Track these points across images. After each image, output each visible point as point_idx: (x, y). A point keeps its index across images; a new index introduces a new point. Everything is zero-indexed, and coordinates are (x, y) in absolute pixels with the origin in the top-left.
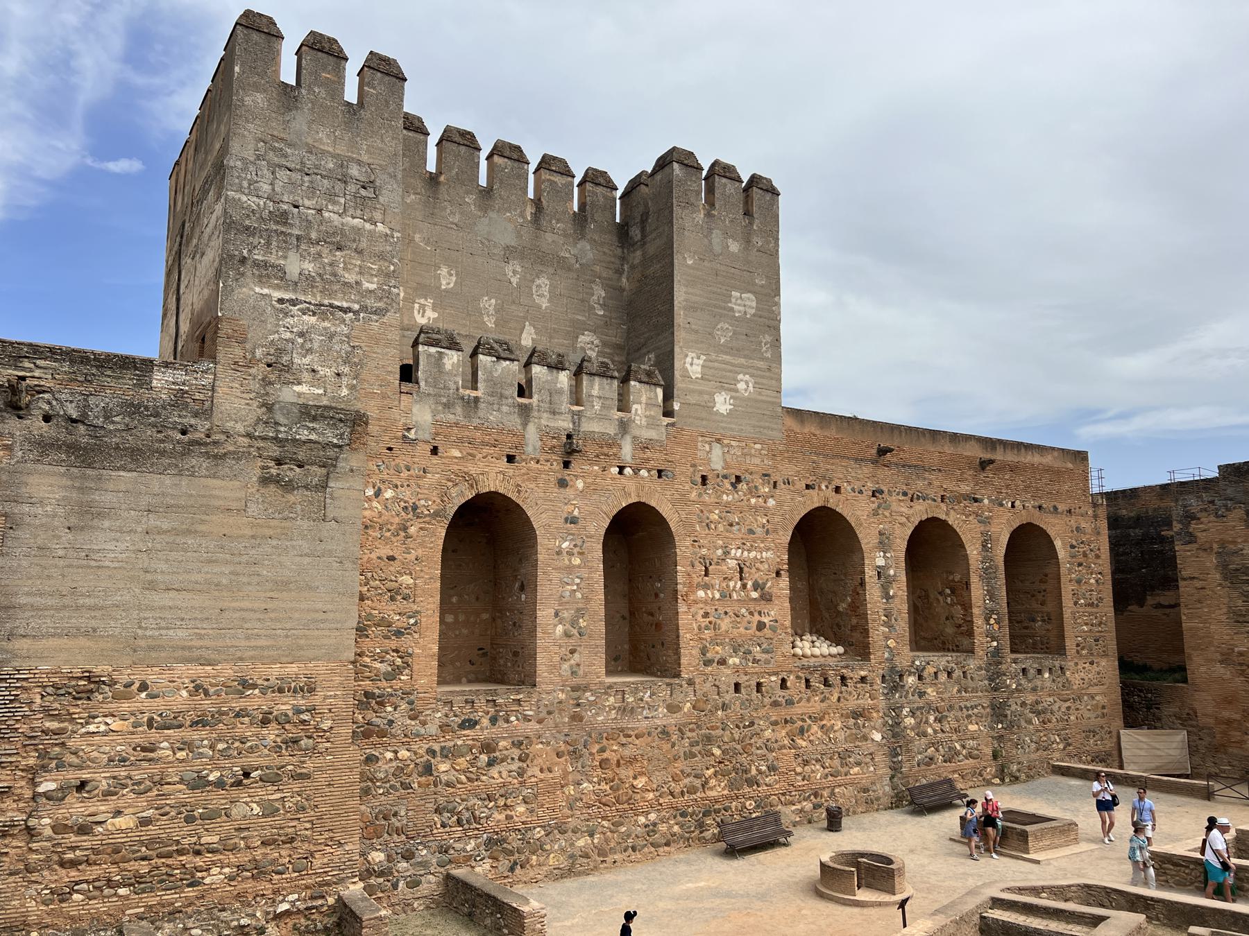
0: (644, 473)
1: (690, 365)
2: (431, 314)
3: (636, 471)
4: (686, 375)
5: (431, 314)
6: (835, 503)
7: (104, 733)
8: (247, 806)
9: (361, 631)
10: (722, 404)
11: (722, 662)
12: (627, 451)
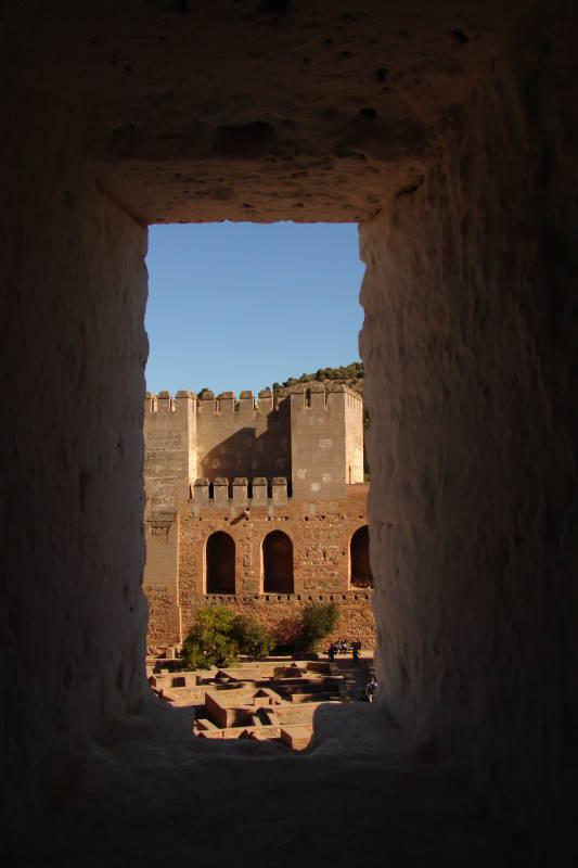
1: (299, 473)
2: (219, 464)
3: (275, 518)
4: (297, 478)
5: (219, 464)
10: (315, 487)
11: (313, 588)
12: (271, 512)
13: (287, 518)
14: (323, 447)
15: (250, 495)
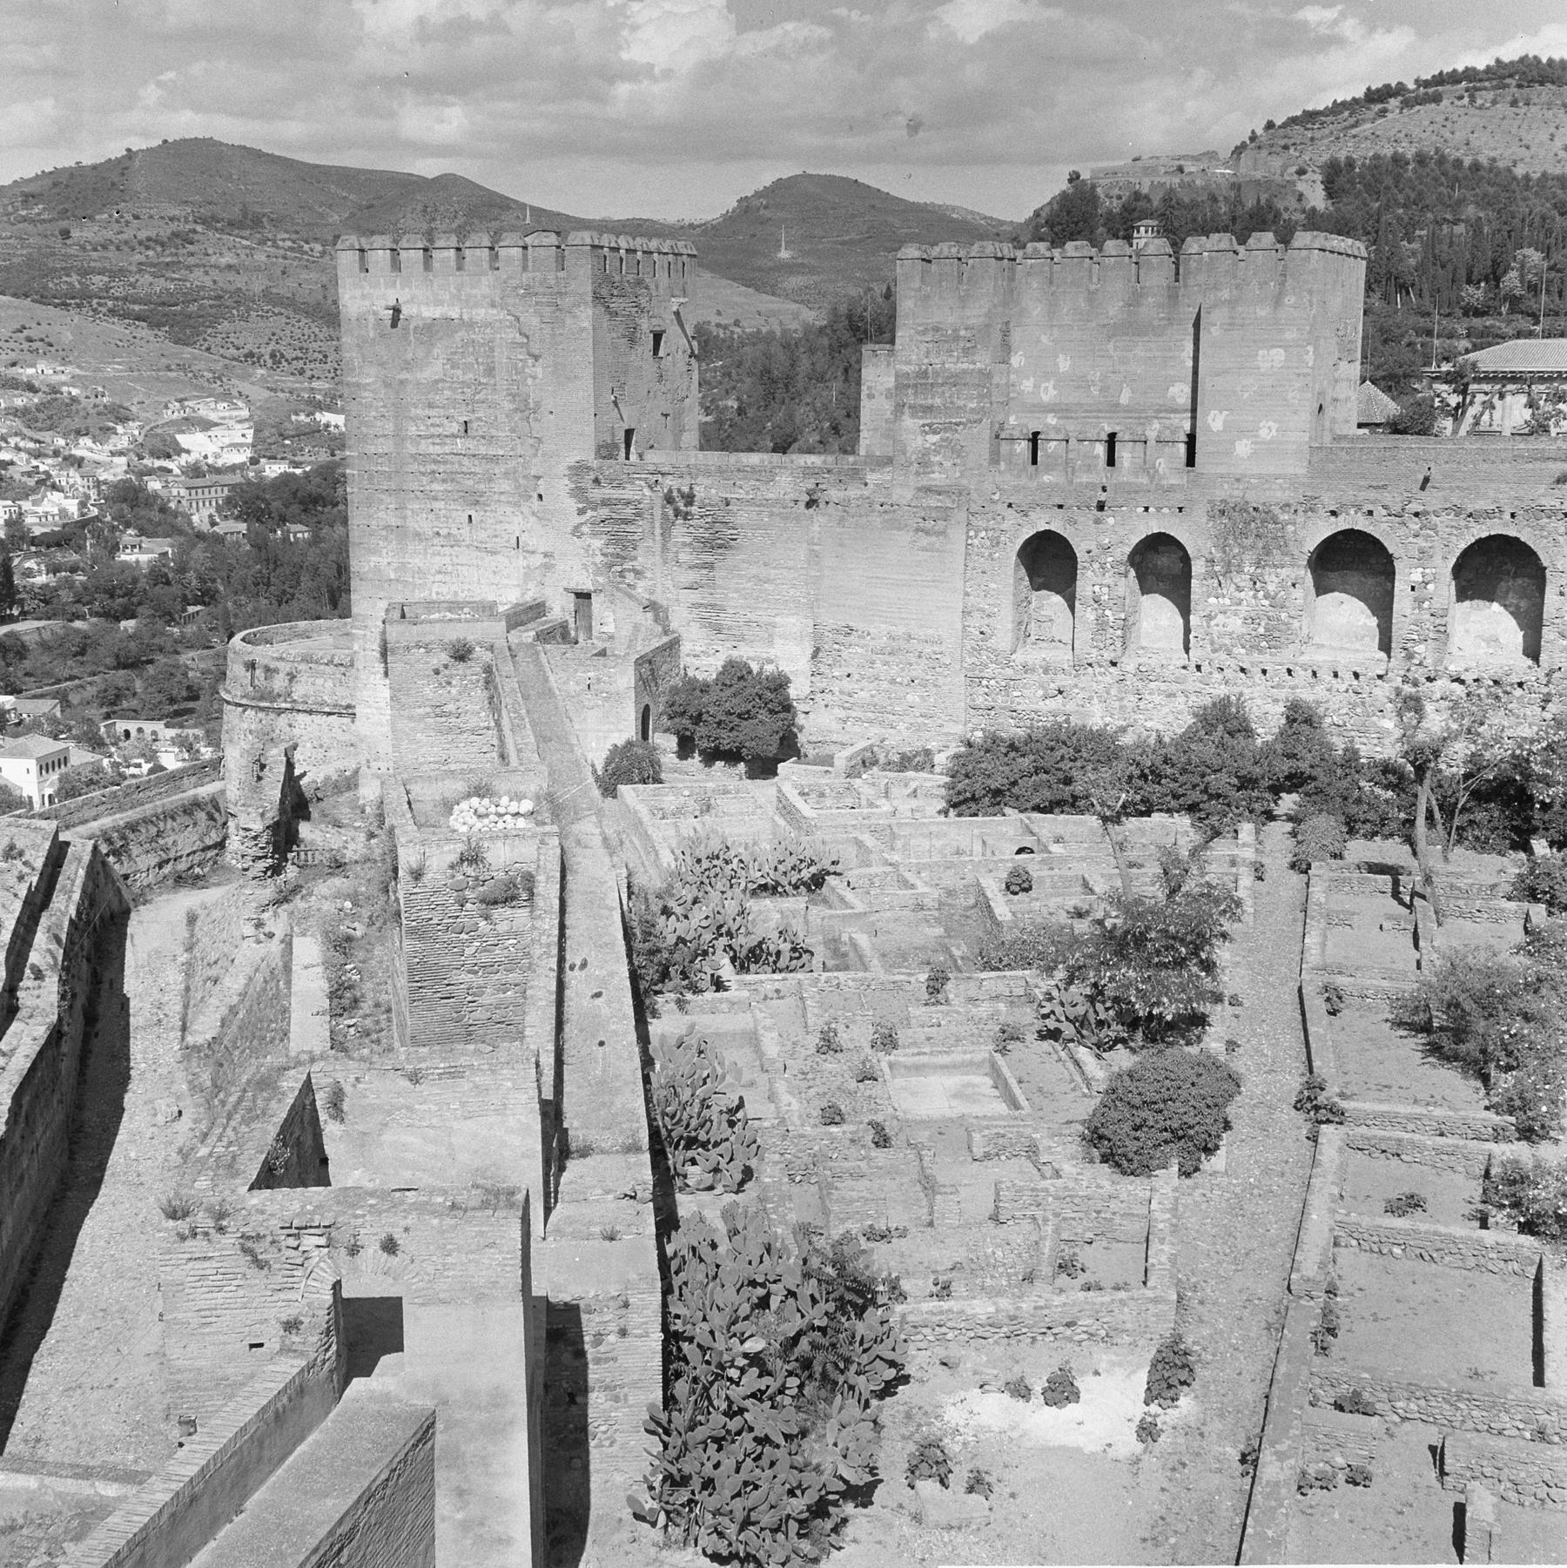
0: (1165, 510)
4: (1209, 429)
6: (1362, 524)
7: (855, 653)
8: (913, 698)
9: (966, 613)
13: (1180, 509)
14: (1265, 366)
15: (1111, 461)
